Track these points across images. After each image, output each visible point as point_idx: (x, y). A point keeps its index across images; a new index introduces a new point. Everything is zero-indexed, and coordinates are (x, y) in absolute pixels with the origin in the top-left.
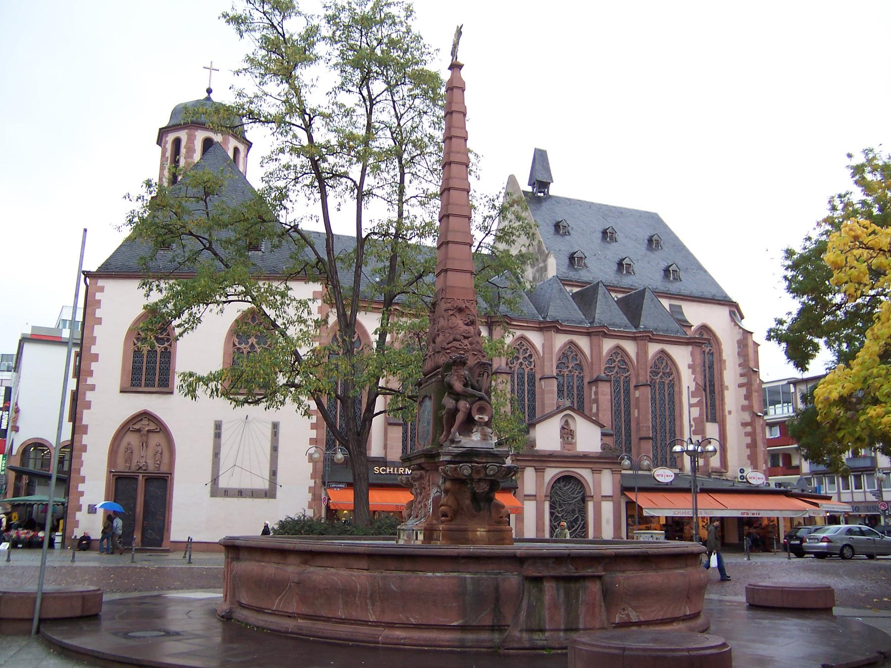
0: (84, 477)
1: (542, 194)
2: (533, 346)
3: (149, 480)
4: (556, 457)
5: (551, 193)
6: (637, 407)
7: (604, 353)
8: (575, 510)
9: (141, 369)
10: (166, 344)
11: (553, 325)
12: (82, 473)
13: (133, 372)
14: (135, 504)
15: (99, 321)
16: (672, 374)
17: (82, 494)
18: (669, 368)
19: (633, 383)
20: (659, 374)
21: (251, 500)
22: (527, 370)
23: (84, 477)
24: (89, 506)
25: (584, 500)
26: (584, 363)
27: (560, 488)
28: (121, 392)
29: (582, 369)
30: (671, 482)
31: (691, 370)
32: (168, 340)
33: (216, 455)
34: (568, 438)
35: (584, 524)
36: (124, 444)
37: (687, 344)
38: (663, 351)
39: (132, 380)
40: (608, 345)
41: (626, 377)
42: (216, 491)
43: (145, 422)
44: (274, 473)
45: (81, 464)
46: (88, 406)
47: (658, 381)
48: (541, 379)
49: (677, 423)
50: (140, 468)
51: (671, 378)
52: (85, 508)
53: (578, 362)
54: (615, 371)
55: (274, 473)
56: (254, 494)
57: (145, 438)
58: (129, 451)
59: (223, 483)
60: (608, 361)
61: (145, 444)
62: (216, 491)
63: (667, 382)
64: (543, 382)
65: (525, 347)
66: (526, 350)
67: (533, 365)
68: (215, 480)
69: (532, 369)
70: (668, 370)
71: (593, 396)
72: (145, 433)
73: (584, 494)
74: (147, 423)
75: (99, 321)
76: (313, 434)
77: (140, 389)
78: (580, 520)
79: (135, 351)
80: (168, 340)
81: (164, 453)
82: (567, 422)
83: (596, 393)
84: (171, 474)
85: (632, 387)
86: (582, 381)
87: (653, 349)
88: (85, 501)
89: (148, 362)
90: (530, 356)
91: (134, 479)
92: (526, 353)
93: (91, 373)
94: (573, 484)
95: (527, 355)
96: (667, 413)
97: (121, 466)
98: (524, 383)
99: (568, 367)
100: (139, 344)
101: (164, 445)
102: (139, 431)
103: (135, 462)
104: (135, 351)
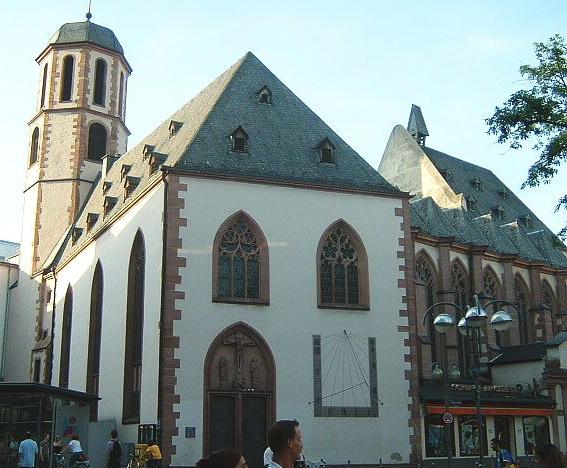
3: (248, 397)
15: (184, 222)
17: (177, 415)
28: (214, 301)
36: (217, 358)
44: (374, 391)
45: (175, 381)
46: (178, 315)
52: (182, 432)
56: (357, 412)
58: (222, 365)
59: (326, 403)
68: (318, 400)
75: (184, 222)
76: (407, 350)
88: (181, 424)
93: (179, 280)
102: (235, 345)
103: (231, 378)
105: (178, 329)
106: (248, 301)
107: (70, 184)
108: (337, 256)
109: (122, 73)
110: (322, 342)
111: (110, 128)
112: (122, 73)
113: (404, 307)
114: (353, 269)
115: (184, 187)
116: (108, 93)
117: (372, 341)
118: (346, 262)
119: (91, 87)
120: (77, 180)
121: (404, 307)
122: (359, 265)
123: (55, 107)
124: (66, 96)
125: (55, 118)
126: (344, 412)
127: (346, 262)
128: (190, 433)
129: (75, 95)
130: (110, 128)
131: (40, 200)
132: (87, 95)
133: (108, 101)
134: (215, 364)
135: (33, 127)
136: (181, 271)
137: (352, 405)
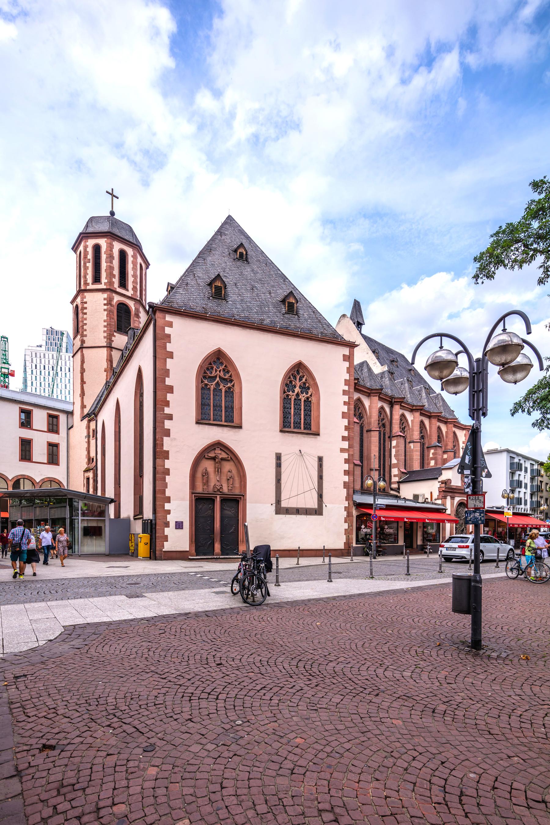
10: (229, 385)
12: (168, 494)
17: (169, 512)
21: (305, 516)
24: (176, 522)
32: (231, 381)
43: (218, 451)
45: (166, 486)
46: (167, 433)
52: (172, 525)
55: (320, 496)
56: (307, 512)
58: (206, 474)
64: (412, 445)
74: (220, 452)
77: (211, 422)
84: (243, 496)
88: (171, 519)
91: (212, 501)
93: (167, 404)
97: (200, 489)
100: (206, 382)
101: (234, 472)
102: (214, 459)
103: (212, 484)
104: (202, 388)
105: (167, 444)
106: (226, 424)
107: (105, 349)
108: (296, 391)
109: (141, 265)
110: (283, 459)
111: (133, 308)
112: (141, 265)
113: (346, 434)
114: (308, 401)
115: (170, 325)
116: (130, 279)
117: (320, 459)
118: (303, 397)
119: (116, 272)
120: (110, 347)
121: (346, 434)
122: (313, 399)
123: (88, 288)
124: (97, 279)
125: (88, 296)
126: (298, 511)
127: (303, 397)
128: (179, 525)
129: (104, 279)
130: (133, 308)
131: (83, 362)
132: (114, 280)
133: (130, 286)
134: (199, 475)
135: (75, 305)
137: (304, 507)
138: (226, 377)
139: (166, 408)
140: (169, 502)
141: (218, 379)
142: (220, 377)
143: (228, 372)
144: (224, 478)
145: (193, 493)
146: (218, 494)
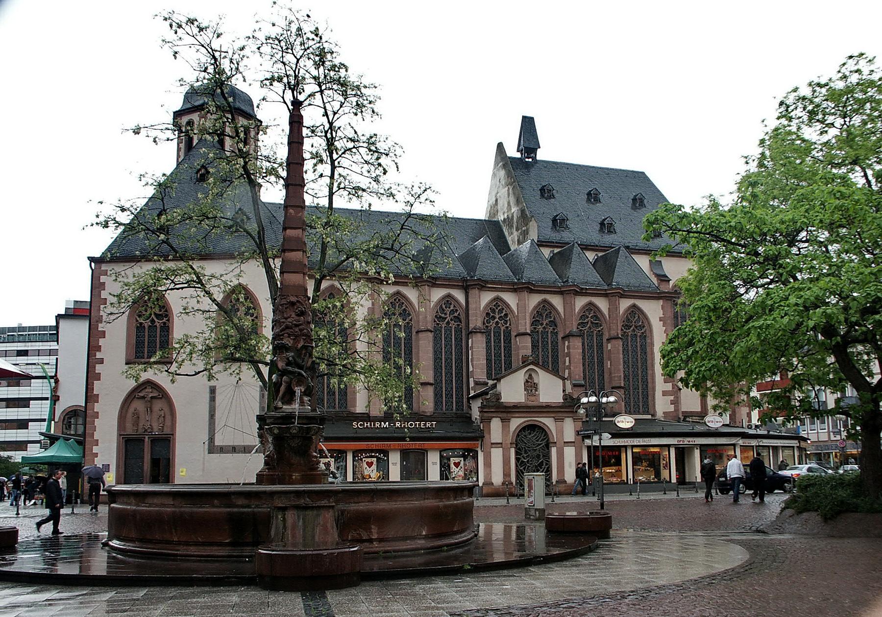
0: (97, 440)
1: (530, 160)
2: (508, 306)
3: (154, 441)
4: (519, 408)
5: (538, 158)
6: (610, 359)
7: (577, 311)
8: (540, 455)
9: (143, 342)
11: (526, 286)
13: (136, 345)
14: (143, 462)
16: (644, 327)
17: (96, 455)
18: (641, 322)
19: (606, 336)
20: (631, 327)
22: (502, 328)
23: (97, 440)
25: (548, 446)
26: (558, 321)
27: (525, 436)
29: (556, 326)
30: (632, 427)
31: (662, 322)
33: (212, 416)
34: (531, 390)
35: (548, 468)
36: (131, 410)
37: (658, 298)
38: (634, 306)
39: (136, 353)
40: (580, 302)
41: (599, 331)
42: (213, 448)
47: (630, 334)
48: (516, 336)
49: (650, 372)
50: (146, 430)
51: (642, 331)
53: (552, 319)
54: (589, 326)
57: (149, 403)
58: (137, 416)
59: (218, 442)
60: (581, 317)
61: (149, 410)
62: (213, 448)
63: (639, 334)
65: (500, 307)
66: (501, 311)
67: (508, 324)
68: (211, 439)
69: (507, 327)
70: (640, 323)
71: (566, 351)
72: (149, 399)
73: (548, 440)
78: (545, 464)
79: (138, 327)
80: (166, 316)
81: (167, 416)
82: (530, 375)
83: (568, 347)
84: (173, 435)
85: (605, 340)
86: (557, 336)
87: (625, 304)
89: (149, 336)
90: (506, 315)
91: (142, 441)
92: (502, 312)
93: (99, 348)
94: (537, 432)
95: (503, 315)
96: (640, 365)
97: (130, 430)
98: (500, 340)
99: (542, 324)
102: (143, 398)
103: (141, 425)
104: (138, 327)
110: (217, 391)
136: (101, 342)
138: (161, 313)
139: (97, 353)
140: (97, 445)
141: (153, 316)
142: (155, 314)
143: (164, 307)
144: (155, 416)
145: (120, 435)
146: (147, 435)
